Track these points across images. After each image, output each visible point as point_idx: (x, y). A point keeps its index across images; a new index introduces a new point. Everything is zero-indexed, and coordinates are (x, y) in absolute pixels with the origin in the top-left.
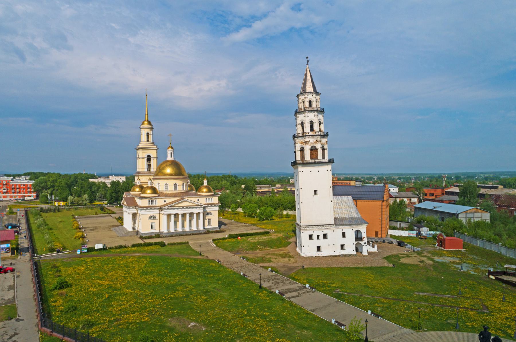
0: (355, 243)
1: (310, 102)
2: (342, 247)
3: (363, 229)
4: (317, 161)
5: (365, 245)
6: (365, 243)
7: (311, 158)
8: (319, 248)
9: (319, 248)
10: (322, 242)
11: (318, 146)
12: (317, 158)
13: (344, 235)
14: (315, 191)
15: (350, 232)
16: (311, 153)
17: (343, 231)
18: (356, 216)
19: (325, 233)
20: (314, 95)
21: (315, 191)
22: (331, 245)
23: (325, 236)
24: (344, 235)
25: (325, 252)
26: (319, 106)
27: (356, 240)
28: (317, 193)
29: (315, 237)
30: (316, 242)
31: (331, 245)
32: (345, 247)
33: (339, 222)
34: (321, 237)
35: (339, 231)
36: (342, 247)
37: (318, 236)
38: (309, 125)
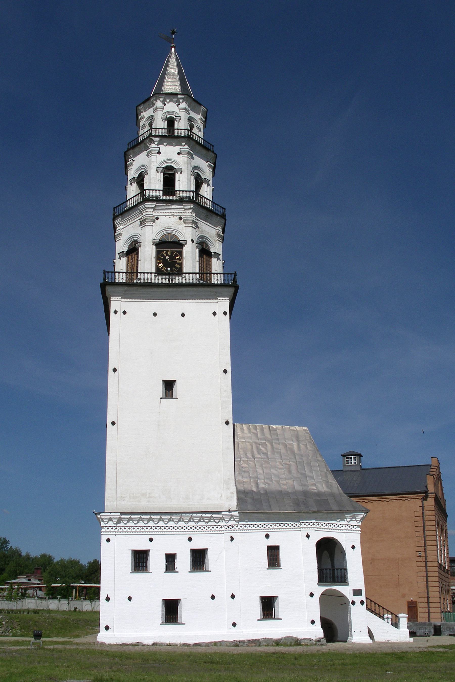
0: (319, 590)
1: (171, 122)
2: (268, 606)
3: (348, 535)
4: (177, 280)
5: (357, 599)
6: (357, 592)
7: (159, 272)
8: (171, 611)
9: (171, 611)
10: (183, 584)
11: (186, 234)
12: (180, 272)
13: (274, 556)
14: (169, 385)
15: (299, 543)
16: (158, 253)
17: (272, 542)
18: (323, 488)
19: (197, 544)
20: (183, 105)
21: (169, 385)
22: (223, 597)
23: (199, 559)
24: (274, 556)
25: (198, 629)
26: (198, 133)
27: (322, 580)
28: (177, 389)
29: (156, 561)
30: (158, 584)
31: (223, 597)
32: (280, 607)
33: (255, 506)
34: (184, 561)
35: (253, 540)
36: (268, 606)
37: (170, 559)
38: (160, 176)
